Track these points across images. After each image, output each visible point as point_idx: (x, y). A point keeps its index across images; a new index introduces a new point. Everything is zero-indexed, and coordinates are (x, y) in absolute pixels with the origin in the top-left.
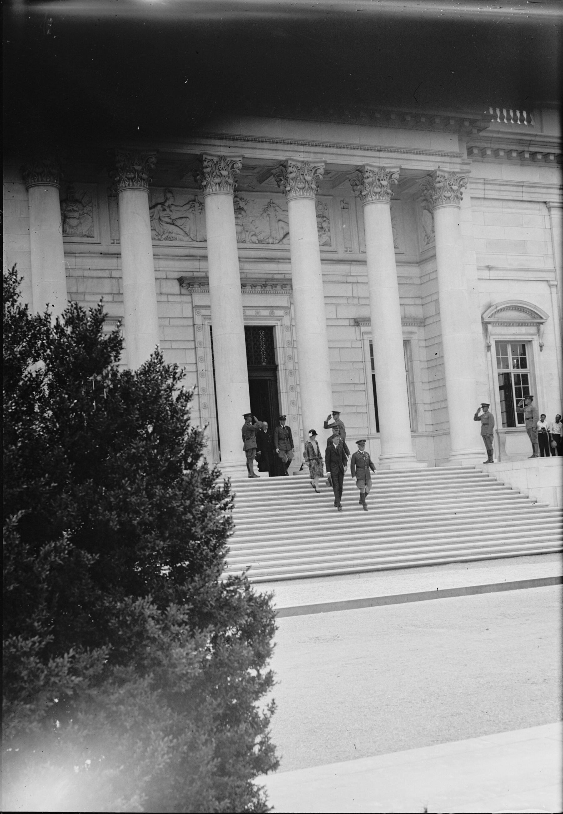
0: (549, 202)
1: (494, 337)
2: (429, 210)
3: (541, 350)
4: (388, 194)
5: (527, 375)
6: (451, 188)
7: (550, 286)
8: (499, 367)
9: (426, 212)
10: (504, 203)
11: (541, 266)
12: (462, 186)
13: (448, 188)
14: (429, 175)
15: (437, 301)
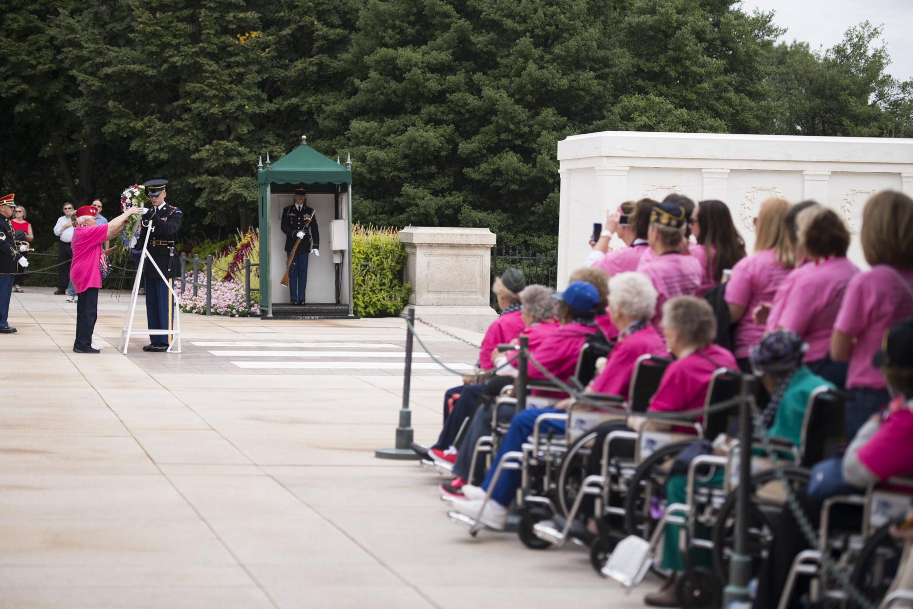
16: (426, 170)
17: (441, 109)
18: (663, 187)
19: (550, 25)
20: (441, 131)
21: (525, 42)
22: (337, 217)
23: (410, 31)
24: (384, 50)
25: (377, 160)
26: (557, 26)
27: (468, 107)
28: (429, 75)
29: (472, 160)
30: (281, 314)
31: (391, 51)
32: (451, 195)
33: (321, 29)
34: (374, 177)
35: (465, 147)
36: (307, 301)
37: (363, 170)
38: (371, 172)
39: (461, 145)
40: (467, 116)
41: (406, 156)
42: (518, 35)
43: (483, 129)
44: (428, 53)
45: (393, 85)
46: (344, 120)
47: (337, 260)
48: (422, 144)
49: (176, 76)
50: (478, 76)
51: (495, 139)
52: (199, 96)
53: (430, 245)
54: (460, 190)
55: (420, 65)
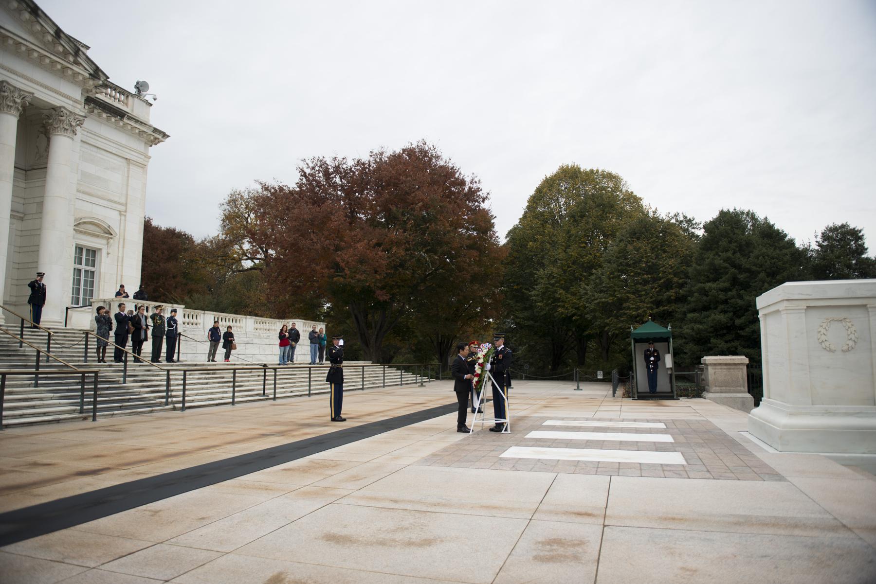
0: (130, 160)
1: (77, 240)
2: (45, 135)
3: (107, 257)
4: (19, 110)
5: (93, 273)
6: (70, 124)
7: (121, 215)
8: (75, 263)
9: (42, 136)
10: (99, 151)
11: (116, 199)
12: (78, 125)
13: (68, 122)
14: (53, 109)
15: (41, 204)
16: (721, 332)
17: (727, 306)
18: (835, 319)
19: (773, 267)
20: (727, 315)
21: (762, 275)
22: (669, 353)
23: (711, 276)
24: (700, 285)
25: (699, 329)
26: (777, 267)
27: (738, 305)
28: (720, 293)
29: (742, 328)
30: (642, 397)
31: (703, 285)
32: (733, 342)
33: (676, 279)
34: (698, 336)
35: (738, 322)
36: (657, 391)
37: (694, 334)
38: (697, 334)
39: (736, 321)
40: (738, 308)
41: (712, 327)
42: (759, 272)
43: (746, 314)
44: (719, 284)
45: (705, 298)
46: (685, 314)
47: (669, 372)
48: (718, 321)
49: (621, 301)
50: (742, 292)
51: (752, 318)
52: (629, 308)
53: (715, 365)
54: (738, 340)
55: (716, 289)
